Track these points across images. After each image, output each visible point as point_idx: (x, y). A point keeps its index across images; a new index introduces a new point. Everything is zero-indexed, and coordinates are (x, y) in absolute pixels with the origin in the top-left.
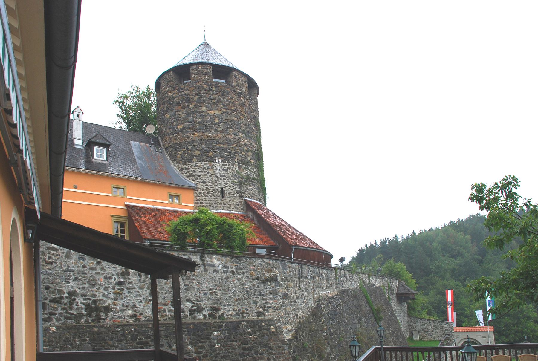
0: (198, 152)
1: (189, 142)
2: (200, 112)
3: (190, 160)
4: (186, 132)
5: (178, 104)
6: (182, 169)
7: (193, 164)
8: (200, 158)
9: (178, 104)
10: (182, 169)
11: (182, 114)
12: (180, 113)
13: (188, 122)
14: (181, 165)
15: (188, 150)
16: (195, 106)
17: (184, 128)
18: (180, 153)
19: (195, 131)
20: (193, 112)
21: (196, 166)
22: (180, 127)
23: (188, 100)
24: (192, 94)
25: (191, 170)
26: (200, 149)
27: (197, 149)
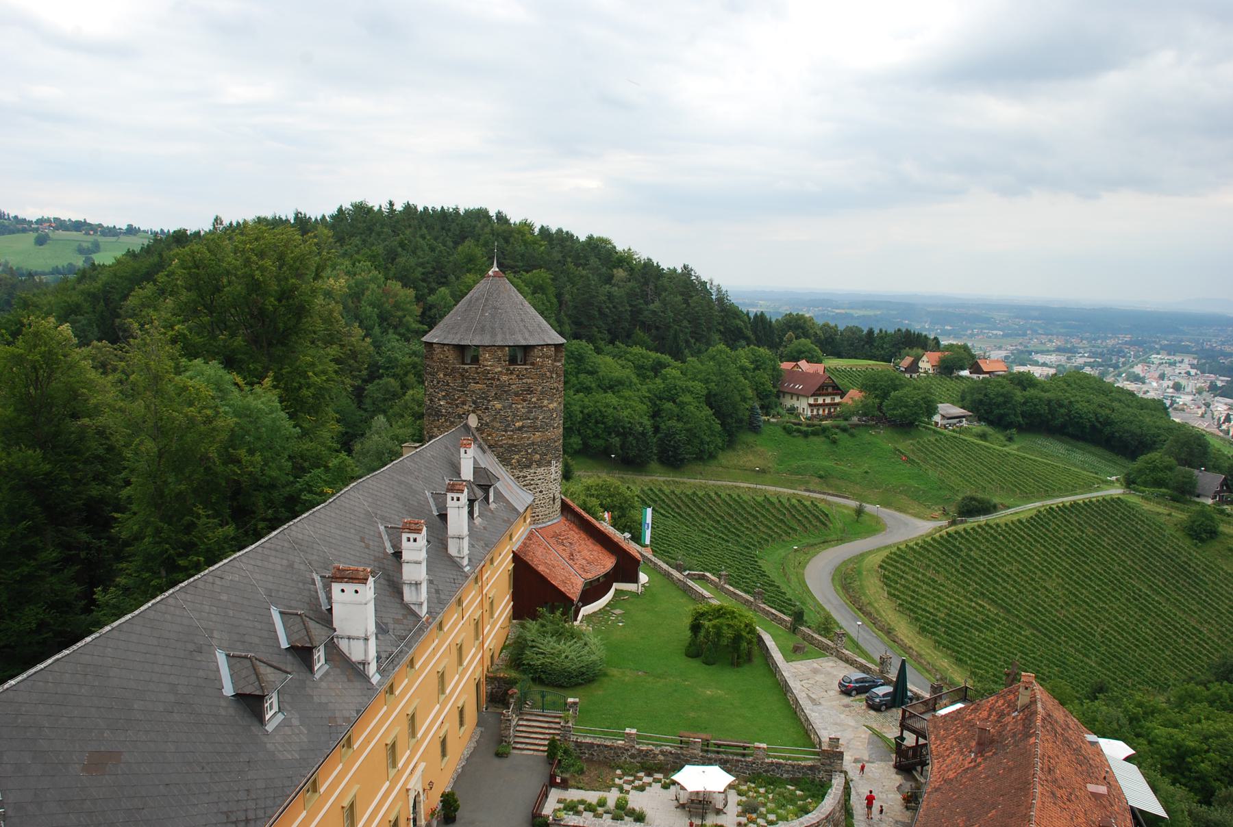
0: (538, 456)
1: (528, 445)
2: (542, 407)
3: (529, 467)
4: (527, 432)
5: (517, 394)
6: (518, 478)
7: (532, 471)
8: (539, 466)
9: (517, 394)
10: (518, 478)
11: (522, 408)
12: (519, 406)
13: (529, 419)
14: (517, 472)
15: (528, 453)
16: (537, 400)
17: (523, 427)
18: (517, 457)
19: (536, 429)
20: (535, 407)
21: (535, 473)
22: (518, 424)
23: (530, 391)
24: (535, 384)
25: (529, 477)
26: (540, 452)
27: (536, 453)
